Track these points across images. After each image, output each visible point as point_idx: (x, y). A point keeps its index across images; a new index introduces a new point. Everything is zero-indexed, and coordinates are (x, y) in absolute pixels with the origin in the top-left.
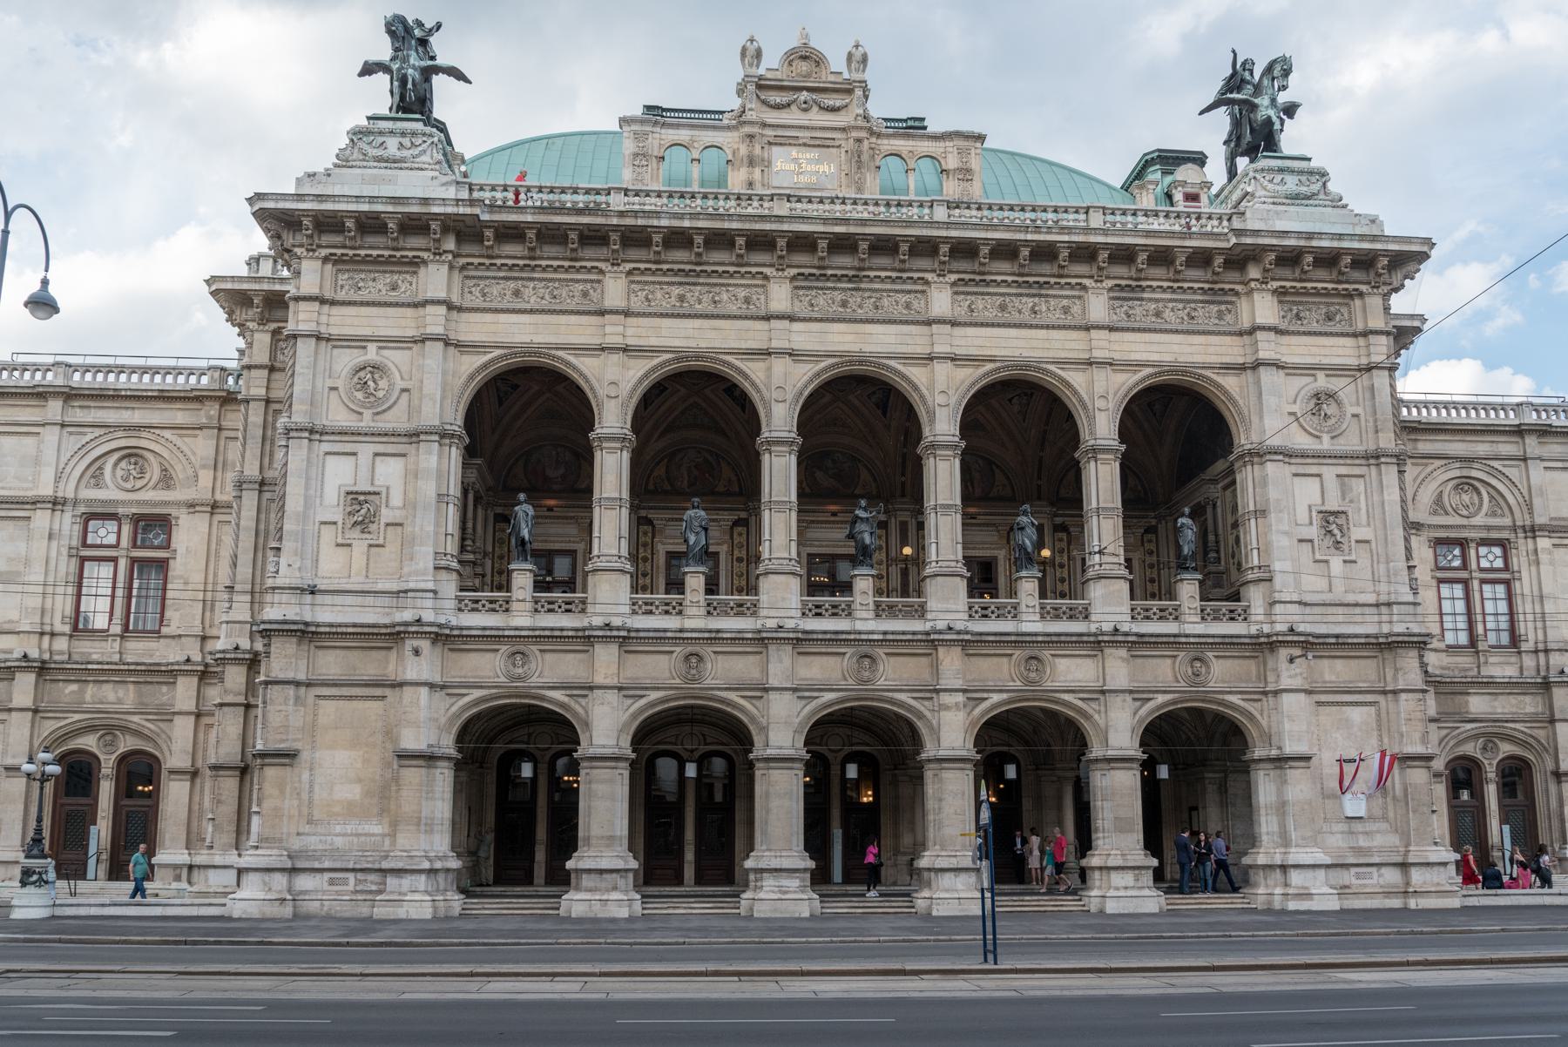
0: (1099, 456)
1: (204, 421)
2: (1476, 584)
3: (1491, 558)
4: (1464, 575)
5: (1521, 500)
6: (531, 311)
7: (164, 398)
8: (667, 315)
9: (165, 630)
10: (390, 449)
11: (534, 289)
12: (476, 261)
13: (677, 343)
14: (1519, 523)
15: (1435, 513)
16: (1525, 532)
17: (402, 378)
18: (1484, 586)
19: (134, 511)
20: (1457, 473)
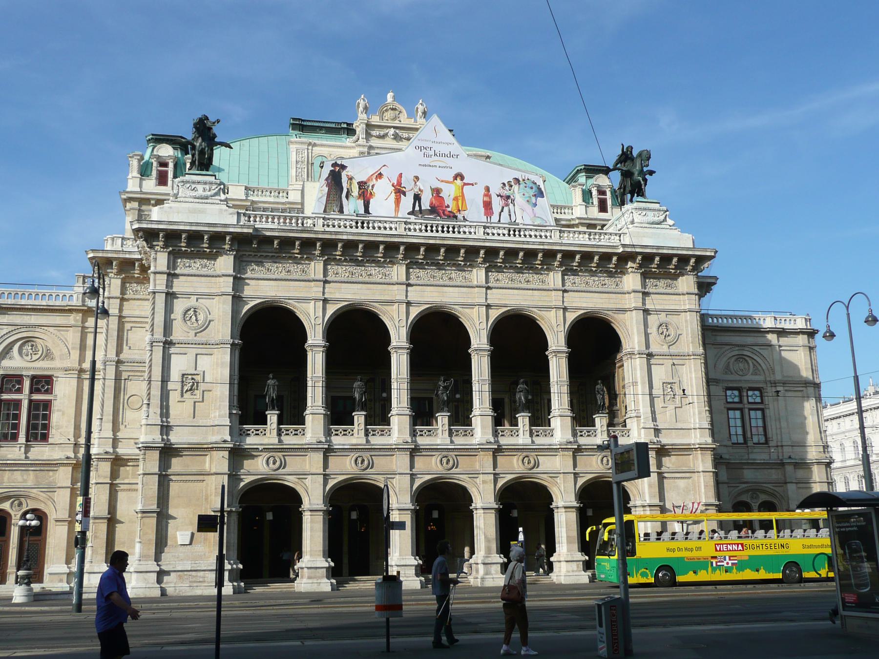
0: (558, 355)
2: (746, 411)
3: (754, 397)
4: (740, 406)
6: (276, 280)
7: (49, 309)
8: (344, 282)
9: (51, 440)
10: (204, 351)
11: (277, 267)
12: (247, 253)
13: (349, 297)
14: (768, 379)
15: (726, 373)
16: (771, 384)
17: (210, 314)
18: (751, 412)
20: (737, 353)
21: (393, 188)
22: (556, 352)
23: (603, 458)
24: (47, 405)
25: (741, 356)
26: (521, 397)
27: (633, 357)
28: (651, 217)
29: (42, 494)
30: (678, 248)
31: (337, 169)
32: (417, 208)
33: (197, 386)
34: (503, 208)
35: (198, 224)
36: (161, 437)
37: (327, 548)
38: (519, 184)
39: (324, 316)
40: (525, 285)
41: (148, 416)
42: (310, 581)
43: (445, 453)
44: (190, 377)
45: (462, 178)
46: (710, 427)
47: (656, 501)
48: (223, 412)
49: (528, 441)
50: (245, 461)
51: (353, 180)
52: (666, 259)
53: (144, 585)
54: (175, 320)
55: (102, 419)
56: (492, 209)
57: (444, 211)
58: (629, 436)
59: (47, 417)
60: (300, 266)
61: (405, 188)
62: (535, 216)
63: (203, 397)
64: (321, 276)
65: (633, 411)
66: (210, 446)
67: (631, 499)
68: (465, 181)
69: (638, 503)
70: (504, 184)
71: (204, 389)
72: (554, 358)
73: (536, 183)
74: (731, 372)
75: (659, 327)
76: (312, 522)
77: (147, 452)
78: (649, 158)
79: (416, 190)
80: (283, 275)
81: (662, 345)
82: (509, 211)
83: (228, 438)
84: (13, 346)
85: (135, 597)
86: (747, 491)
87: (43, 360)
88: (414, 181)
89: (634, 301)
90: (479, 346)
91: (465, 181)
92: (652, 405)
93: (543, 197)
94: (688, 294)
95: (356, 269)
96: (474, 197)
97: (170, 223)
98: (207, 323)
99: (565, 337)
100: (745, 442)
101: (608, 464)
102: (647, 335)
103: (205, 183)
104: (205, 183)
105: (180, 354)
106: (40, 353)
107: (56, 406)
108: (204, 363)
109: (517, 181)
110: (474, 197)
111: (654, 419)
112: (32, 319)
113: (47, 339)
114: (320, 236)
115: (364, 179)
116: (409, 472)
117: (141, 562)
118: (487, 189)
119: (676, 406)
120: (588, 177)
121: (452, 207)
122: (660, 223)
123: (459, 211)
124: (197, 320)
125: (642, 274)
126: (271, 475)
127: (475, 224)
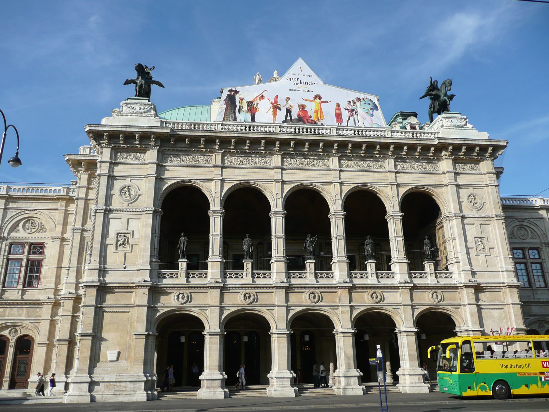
0: (394, 218)
1: (59, 207)
2: (529, 264)
3: (533, 254)
5: (542, 233)
6: (187, 166)
7: (45, 198)
8: (237, 168)
10: (134, 216)
12: (167, 149)
14: (543, 241)
16: (545, 245)
17: (139, 190)
18: (532, 265)
19: (30, 241)
20: (518, 223)
21: (272, 105)
22: (393, 216)
23: (433, 294)
24: (39, 263)
25: (521, 226)
26: (368, 248)
27: (451, 219)
28: (455, 122)
29: (31, 324)
30: (479, 140)
31: (233, 93)
32: (289, 118)
33: (128, 241)
34: (349, 117)
35: (131, 127)
36: (98, 278)
37: (222, 364)
38: (361, 102)
39: (222, 191)
40: (368, 169)
41: (90, 263)
42: (208, 390)
43: (312, 291)
44: (123, 235)
45: (320, 98)
46: (514, 270)
47: (478, 327)
48: (145, 260)
49: (375, 281)
50: (161, 297)
51: (243, 100)
52: (470, 148)
53: (78, 393)
54: (114, 194)
55: (69, 270)
56: (342, 118)
57: (308, 120)
58: (451, 277)
59: (39, 271)
60: (205, 157)
61: (280, 105)
62: (373, 123)
63: (132, 250)
64: (220, 163)
65: (454, 259)
66: (134, 285)
67: (457, 326)
68: (322, 100)
69: (463, 328)
70: (350, 102)
71: (133, 244)
72: (392, 220)
73: (372, 101)
74: (515, 236)
75: (468, 198)
76: (210, 343)
77: (87, 289)
78: (451, 85)
79: (288, 106)
80: (193, 163)
81: (472, 210)
82: (354, 120)
83: (148, 279)
84: (19, 223)
85: (70, 402)
86: (535, 322)
87: (39, 232)
88: (286, 100)
89: (448, 178)
90: (336, 211)
91: (322, 100)
92: (468, 254)
93: (378, 110)
94: (488, 173)
95: (245, 159)
96: (329, 111)
97: (111, 126)
98: (137, 197)
99: (399, 205)
100: (530, 286)
101: (437, 299)
102: (460, 203)
103: (141, 104)
104: (141, 104)
105: (117, 218)
106: (37, 227)
107: (45, 263)
108: (134, 225)
109: (359, 99)
110: (329, 111)
111: (470, 265)
112: (33, 205)
113: (42, 218)
114: (219, 135)
115: (251, 100)
116: (285, 304)
117: (78, 375)
118: (338, 105)
119: (487, 254)
120: (403, 120)
121: (314, 117)
122: (462, 126)
123: (319, 119)
124: (130, 195)
125: (453, 160)
126: (181, 307)
127: (330, 127)
